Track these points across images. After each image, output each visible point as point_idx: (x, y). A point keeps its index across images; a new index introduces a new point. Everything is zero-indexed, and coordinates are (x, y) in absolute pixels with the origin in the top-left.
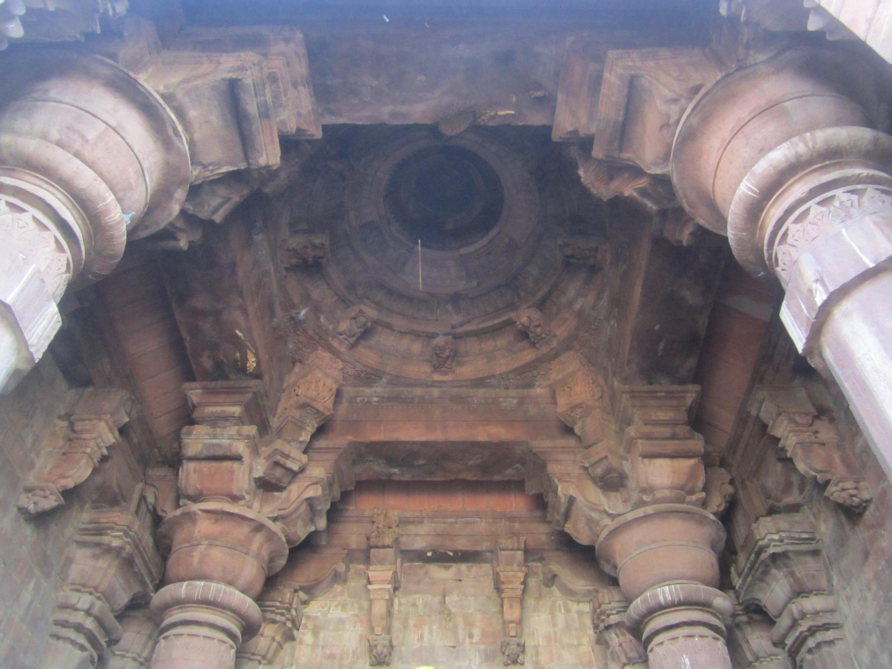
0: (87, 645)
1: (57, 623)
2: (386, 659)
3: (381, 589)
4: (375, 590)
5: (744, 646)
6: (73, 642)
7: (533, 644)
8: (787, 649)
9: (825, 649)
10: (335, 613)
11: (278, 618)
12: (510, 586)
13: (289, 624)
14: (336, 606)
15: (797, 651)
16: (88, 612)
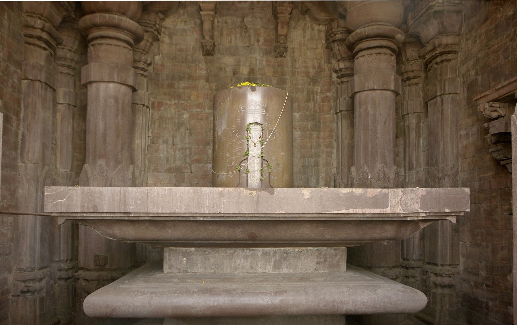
0: (47, 47)
1: (26, 36)
2: (212, 53)
3: (207, 15)
4: (204, 15)
5: (403, 54)
6: (39, 46)
7: (291, 47)
8: (425, 60)
9: (445, 63)
10: (181, 26)
11: (149, 29)
12: (283, 15)
13: (156, 33)
14: (181, 22)
15: (430, 62)
16: (42, 30)
